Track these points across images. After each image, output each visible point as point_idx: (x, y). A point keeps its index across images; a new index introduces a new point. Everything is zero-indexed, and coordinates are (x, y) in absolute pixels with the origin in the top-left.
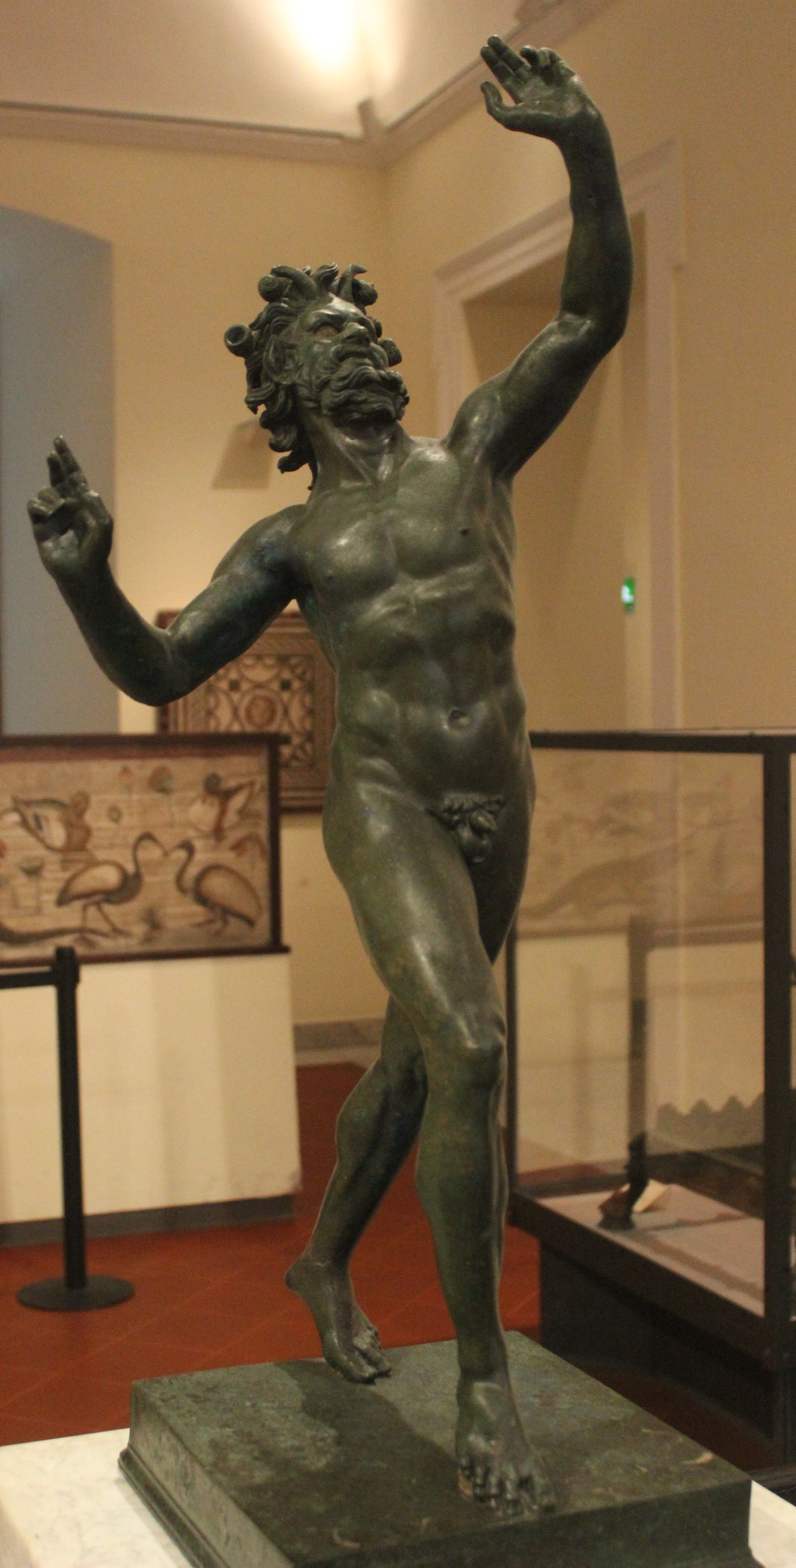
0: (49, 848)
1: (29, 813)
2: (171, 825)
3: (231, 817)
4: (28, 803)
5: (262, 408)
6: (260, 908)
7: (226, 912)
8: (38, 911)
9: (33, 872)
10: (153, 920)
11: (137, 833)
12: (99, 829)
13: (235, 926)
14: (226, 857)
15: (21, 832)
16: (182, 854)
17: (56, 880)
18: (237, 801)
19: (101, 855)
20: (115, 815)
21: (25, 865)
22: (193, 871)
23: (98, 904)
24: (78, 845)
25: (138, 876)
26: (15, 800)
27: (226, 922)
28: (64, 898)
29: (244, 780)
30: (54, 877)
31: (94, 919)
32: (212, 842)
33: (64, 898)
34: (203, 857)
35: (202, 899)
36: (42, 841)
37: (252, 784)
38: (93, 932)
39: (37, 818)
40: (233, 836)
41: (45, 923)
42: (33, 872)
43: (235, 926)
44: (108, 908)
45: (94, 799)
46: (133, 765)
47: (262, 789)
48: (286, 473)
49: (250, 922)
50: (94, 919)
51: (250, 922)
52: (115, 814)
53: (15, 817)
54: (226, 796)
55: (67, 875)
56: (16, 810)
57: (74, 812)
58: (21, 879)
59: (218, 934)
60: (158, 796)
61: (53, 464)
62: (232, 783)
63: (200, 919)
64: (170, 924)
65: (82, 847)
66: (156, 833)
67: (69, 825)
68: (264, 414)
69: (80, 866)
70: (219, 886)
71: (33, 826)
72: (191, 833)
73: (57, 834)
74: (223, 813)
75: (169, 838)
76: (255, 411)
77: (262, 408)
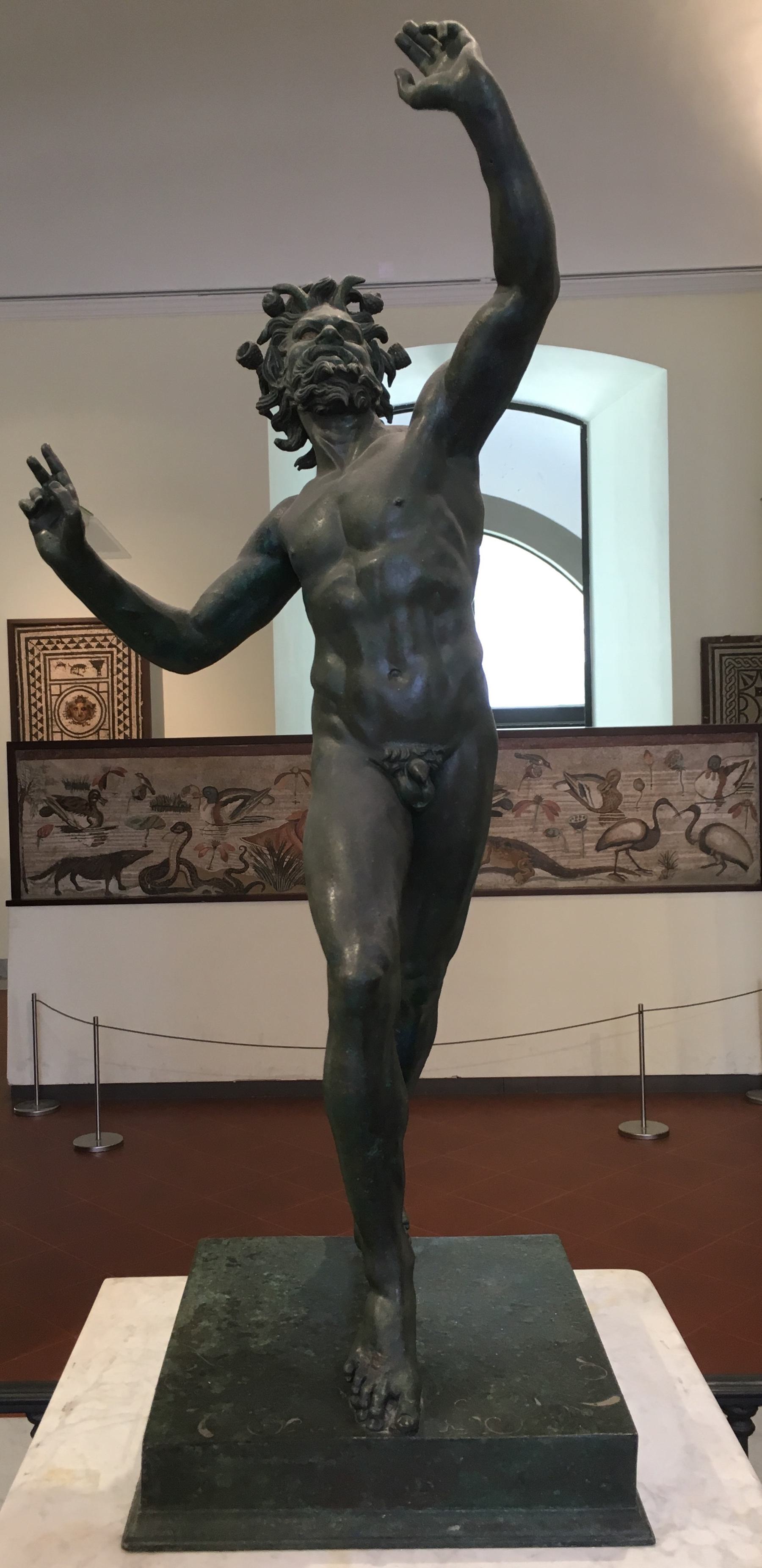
0: (590, 809)
1: (576, 784)
2: (681, 793)
3: (729, 788)
4: (575, 777)
6: (752, 855)
7: (725, 859)
8: (583, 854)
9: (579, 826)
10: (668, 864)
11: (657, 799)
12: (626, 796)
13: (732, 869)
14: (726, 817)
15: (570, 797)
16: (691, 815)
17: (596, 832)
18: (734, 776)
19: (629, 815)
20: (640, 786)
21: (573, 821)
22: (699, 827)
23: (627, 849)
24: (611, 808)
25: (657, 829)
26: (565, 774)
27: (725, 866)
28: (600, 846)
29: (740, 761)
30: (594, 830)
31: (623, 861)
32: (714, 806)
33: (600, 846)
34: (708, 816)
35: (705, 848)
36: (586, 804)
37: (747, 762)
38: (623, 870)
39: (581, 787)
40: (730, 802)
41: (589, 864)
42: (579, 826)
43: (732, 869)
44: (634, 853)
45: (623, 774)
46: (651, 748)
47: (753, 767)
49: (745, 867)
50: (623, 861)
51: (745, 867)
52: (639, 785)
53: (566, 787)
54: (727, 771)
55: (605, 828)
56: (566, 782)
57: (609, 783)
58: (571, 831)
59: (718, 875)
60: (674, 771)
62: (730, 763)
64: (681, 866)
65: (614, 809)
66: (670, 799)
67: (604, 793)
69: (613, 822)
70: (719, 839)
71: (580, 794)
72: (698, 799)
73: (596, 799)
75: (680, 803)
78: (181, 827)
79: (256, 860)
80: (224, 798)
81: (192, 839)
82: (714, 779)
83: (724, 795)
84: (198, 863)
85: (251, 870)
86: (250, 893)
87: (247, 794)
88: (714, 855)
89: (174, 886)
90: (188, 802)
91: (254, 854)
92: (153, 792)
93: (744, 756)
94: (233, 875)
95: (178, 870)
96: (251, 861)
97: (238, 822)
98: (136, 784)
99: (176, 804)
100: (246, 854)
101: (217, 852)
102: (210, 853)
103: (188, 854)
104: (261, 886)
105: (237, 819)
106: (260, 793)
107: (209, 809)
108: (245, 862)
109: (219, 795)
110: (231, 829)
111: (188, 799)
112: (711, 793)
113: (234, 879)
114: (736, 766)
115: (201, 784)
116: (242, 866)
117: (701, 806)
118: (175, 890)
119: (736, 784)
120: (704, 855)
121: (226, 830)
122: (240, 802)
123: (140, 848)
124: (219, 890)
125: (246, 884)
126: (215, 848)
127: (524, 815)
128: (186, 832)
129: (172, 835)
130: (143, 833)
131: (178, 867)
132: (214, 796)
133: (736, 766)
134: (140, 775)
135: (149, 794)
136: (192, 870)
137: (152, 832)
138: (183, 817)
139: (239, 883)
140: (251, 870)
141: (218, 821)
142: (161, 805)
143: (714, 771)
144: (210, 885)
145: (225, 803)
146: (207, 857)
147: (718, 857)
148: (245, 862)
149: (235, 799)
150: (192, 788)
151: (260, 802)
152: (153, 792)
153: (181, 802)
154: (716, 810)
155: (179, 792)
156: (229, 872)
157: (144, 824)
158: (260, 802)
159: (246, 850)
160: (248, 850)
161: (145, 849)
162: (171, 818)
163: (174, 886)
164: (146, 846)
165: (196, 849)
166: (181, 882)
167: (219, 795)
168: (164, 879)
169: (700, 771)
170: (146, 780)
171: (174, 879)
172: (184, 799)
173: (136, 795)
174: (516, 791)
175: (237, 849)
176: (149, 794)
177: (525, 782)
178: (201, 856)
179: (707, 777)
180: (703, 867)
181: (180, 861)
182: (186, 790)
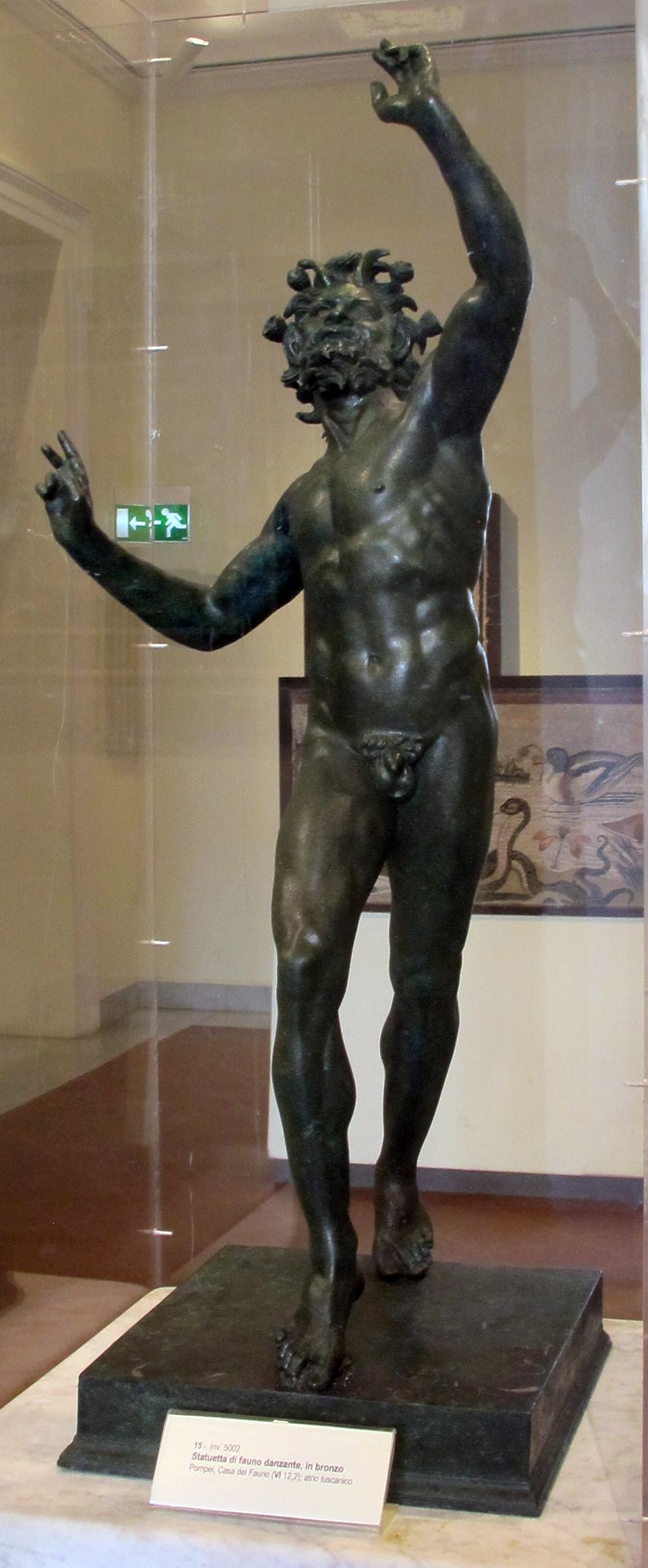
78: (515, 805)
79: (621, 857)
80: (577, 766)
81: (531, 823)
85: (613, 872)
86: (612, 904)
87: (609, 760)
89: (501, 891)
90: (526, 770)
91: (620, 849)
95: (509, 868)
96: (613, 857)
97: (597, 801)
99: (509, 773)
100: (607, 849)
101: (565, 843)
102: (555, 844)
103: (524, 844)
104: (628, 896)
105: (596, 796)
106: (629, 758)
107: (556, 779)
108: (605, 859)
109: (570, 760)
110: (587, 811)
111: (525, 765)
116: (600, 864)
118: (505, 896)
121: (579, 811)
124: (566, 898)
125: (606, 891)
126: (563, 837)
128: (521, 814)
131: (509, 863)
136: (531, 870)
139: (596, 890)
140: (613, 872)
141: (567, 796)
144: (554, 890)
145: (578, 773)
146: (551, 851)
148: (605, 859)
149: (594, 767)
150: (531, 749)
151: (628, 772)
153: (515, 769)
155: (514, 755)
156: (582, 873)
158: (628, 772)
159: (606, 843)
160: (611, 842)
163: (501, 891)
165: (535, 838)
166: (514, 885)
167: (570, 760)
171: (503, 880)
172: (520, 765)
175: (594, 840)
178: (542, 848)
181: (513, 855)
182: (524, 752)
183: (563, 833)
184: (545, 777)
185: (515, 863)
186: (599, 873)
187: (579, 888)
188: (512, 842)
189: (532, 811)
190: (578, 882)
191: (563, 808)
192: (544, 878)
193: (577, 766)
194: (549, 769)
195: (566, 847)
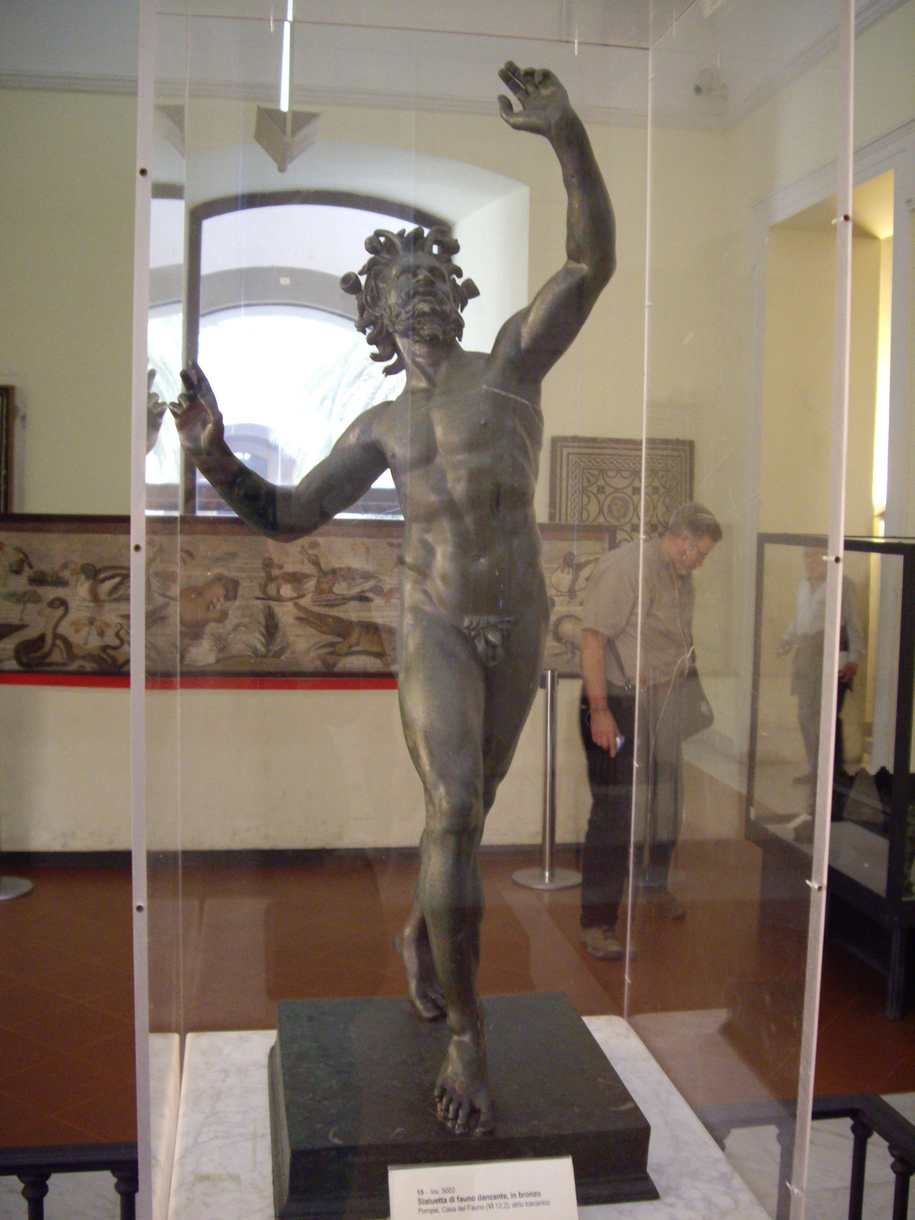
3: (581, 582)
5: (368, 331)
18: (586, 572)
29: (591, 558)
32: (567, 598)
35: (558, 638)
48: (389, 377)
54: (580, 567)
61: (185, 376)
62: (583, 560)
63: (556, 651)
68: (370, 334)
74: (575, 580)
76: (364, 332)
77: (368, 331)
80: (102, 576)
82: (568, 573)
83: (577, 589)
84: (75, 639)
88: (565, 644)
89: (49, 660)
92: (31, 567)
93: (595, 553)
94: (109, 651)
95: (54, 645)
98: (14, 557)
101: (93, 628)
103: (65, 629)
105: (115, 596)
110: (108, 606)
111: (66, 574)
112: (564, 588)
113: (109, 655)
114: (588, 562)
115: (78, 560)
116: (116, 642)
117: (555, 598)
118: (51, 664)
119: (587, 579)
120: (556, 644)
122: (117, 580)
123: (15, 621)
127: (394, 601)
128: (62, 608)
129: (48, 611)
130: (20, 607)
132: (93, 573)
133: (588, 562)
134: (19, 550)
135: (26, 568)
137: (30, 606)
138: (60, 592)
139: (114, 659)
141: (95, 597)
142: (39, 579)
143: (569, 566)
146: (84, 632)
147: (569, 645)
149: (113, 577)
152: (31, 567)
153: (59, 578)
154: (569, 602)
156: (105, 648)
157: (20, 598)
161: (21, 623)
162: (51, 593)
163: (49, 660)
164: (21, 620)
168: (39, 654)
169: (556, 566)
170: (26, 556)
171: (49, 654)
172: (61, 575)
173: (15, 568)
174: (387, 579)
176: (26, 568)
177: (396, 570)
178: (77, 631)
179: (562, 572)
180: (556, 655)
181: (56, 636)
182: (65, 566)
183: (91, 621)
184: (79, 583)
185: (58, 642)
186: (115, 648)
187: (104, 660)
188: (56, 626)
189: (70, 606)
190: (103, 655)
191: (91, 604)
192: (76, 651)
193: (102, 576)
194: (83, 577)
195: (94, 631)
